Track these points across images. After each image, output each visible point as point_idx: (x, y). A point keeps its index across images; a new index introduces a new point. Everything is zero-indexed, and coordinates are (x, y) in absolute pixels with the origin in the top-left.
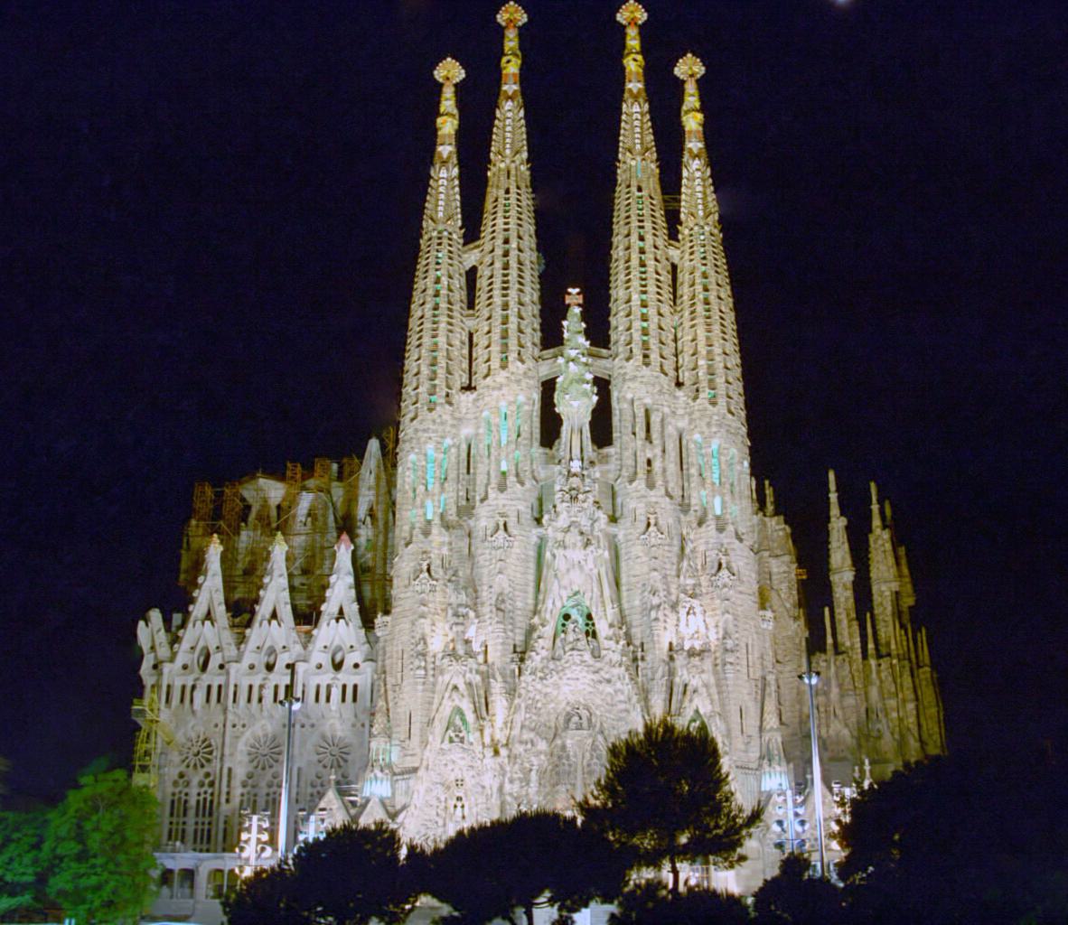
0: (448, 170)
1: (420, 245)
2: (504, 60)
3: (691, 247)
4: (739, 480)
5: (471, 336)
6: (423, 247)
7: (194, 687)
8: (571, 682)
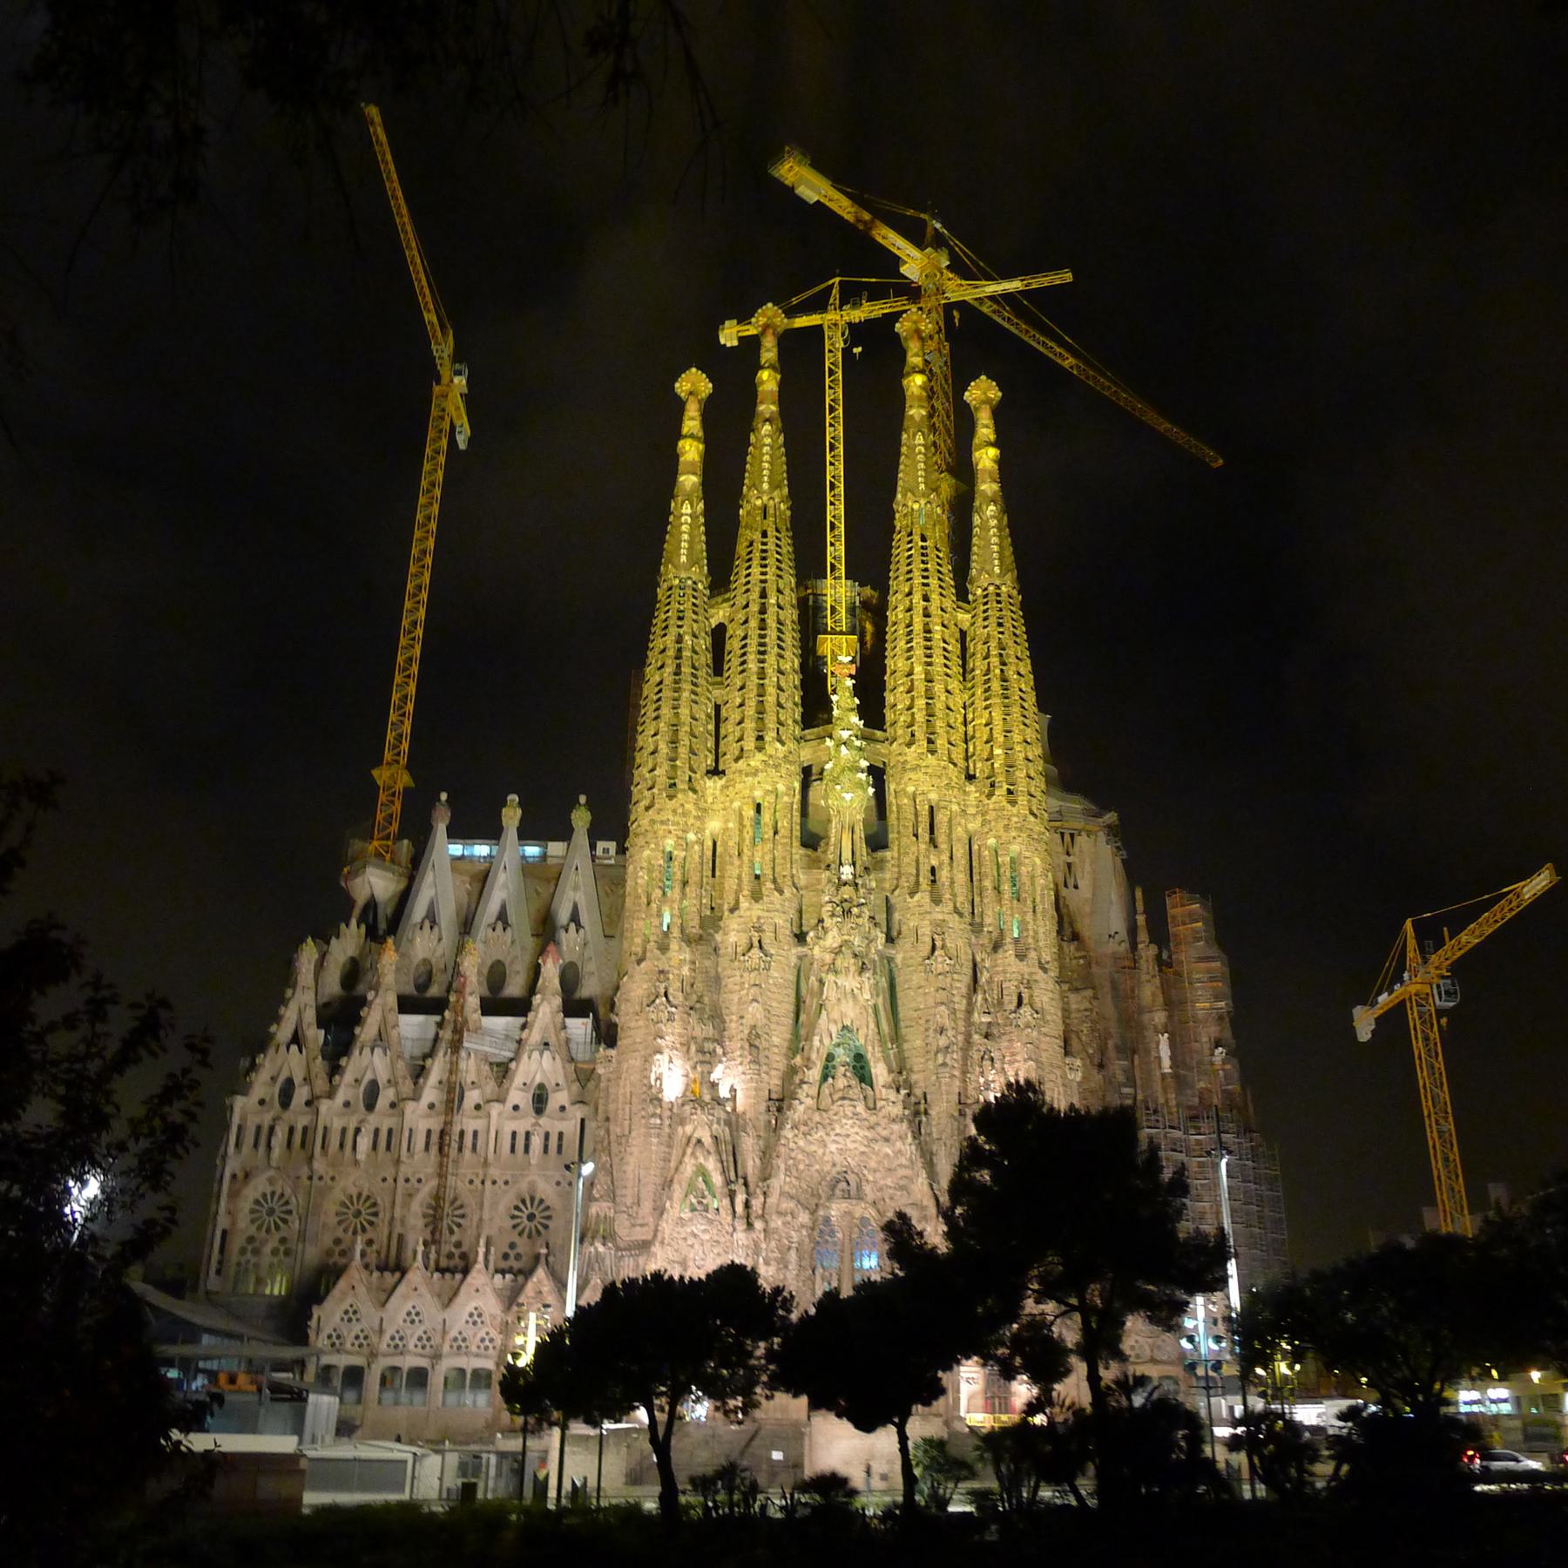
3: (985, 611)
4: (1043, 895)
5: (717, 708)
6: (659, 597)
7: (358, 1131)
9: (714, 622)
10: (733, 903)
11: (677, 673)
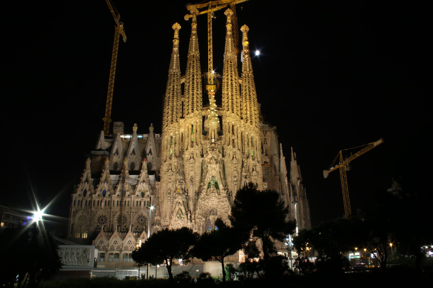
0: (176, 55)
1: (168, 76)
2: (192, 24)
3: (245, 80)
4: (258, 146)
5: (183, 102)
6: (169, 77)
7: (101, 201)
8: (212, 202)
9: (182, 82)
10: (187, 148)
11: (173, 94)
